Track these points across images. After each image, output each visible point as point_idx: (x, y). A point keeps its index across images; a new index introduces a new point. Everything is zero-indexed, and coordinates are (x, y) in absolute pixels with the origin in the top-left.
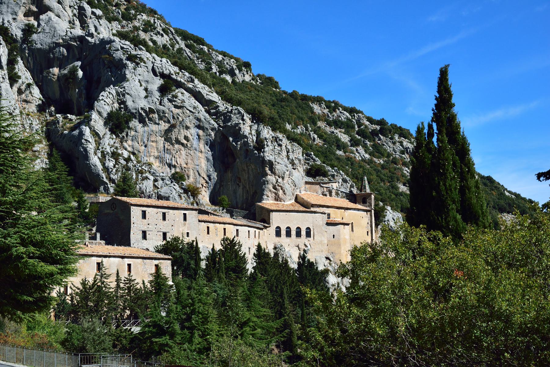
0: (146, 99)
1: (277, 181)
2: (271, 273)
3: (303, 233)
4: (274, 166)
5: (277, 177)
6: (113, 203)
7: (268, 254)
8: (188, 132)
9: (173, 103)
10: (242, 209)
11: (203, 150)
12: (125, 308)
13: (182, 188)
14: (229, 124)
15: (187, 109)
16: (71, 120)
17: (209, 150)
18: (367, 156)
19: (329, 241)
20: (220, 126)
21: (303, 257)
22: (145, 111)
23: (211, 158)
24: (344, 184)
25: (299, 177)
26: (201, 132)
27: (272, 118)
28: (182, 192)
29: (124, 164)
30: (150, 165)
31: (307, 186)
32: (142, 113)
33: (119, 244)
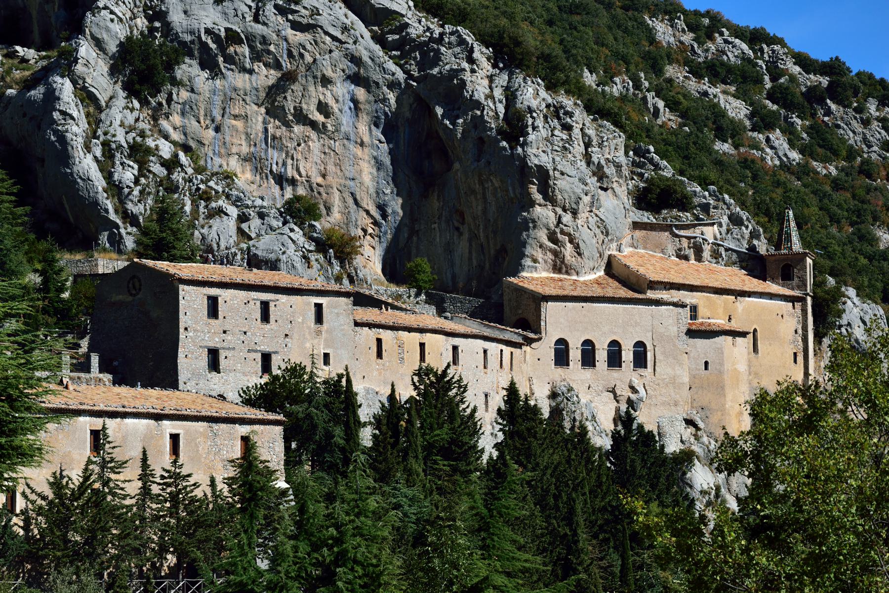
0: (220, 7)
1: (559, 221)
2: (544, 461)
3: (627, 356)
4: (551, 183)
5: (559, 211)
6: (134, 277)
7: (536, 410)
8: (328, 94)
9: (290, 17)
10: (468, 293)
11: (366, 139)
12: (162, 550)
13: (311, 239)
14: (435, 71)
15: (327, 33)
16: (24, 60)
17: (383, 139)
18: (795, 156)
19: (693, 377)
20: (410, 76)
21: (625, 420)
22: (216, 38)
23: (387, 161)
24: (736, 230)
25: (617, 212)
26: (361, 93)
27: (546, 58)
28: (312, 248)
29: (162, 175)
30: (228, 177)
31: (638, 234)
32: (209, 41)
33: (149, 383)
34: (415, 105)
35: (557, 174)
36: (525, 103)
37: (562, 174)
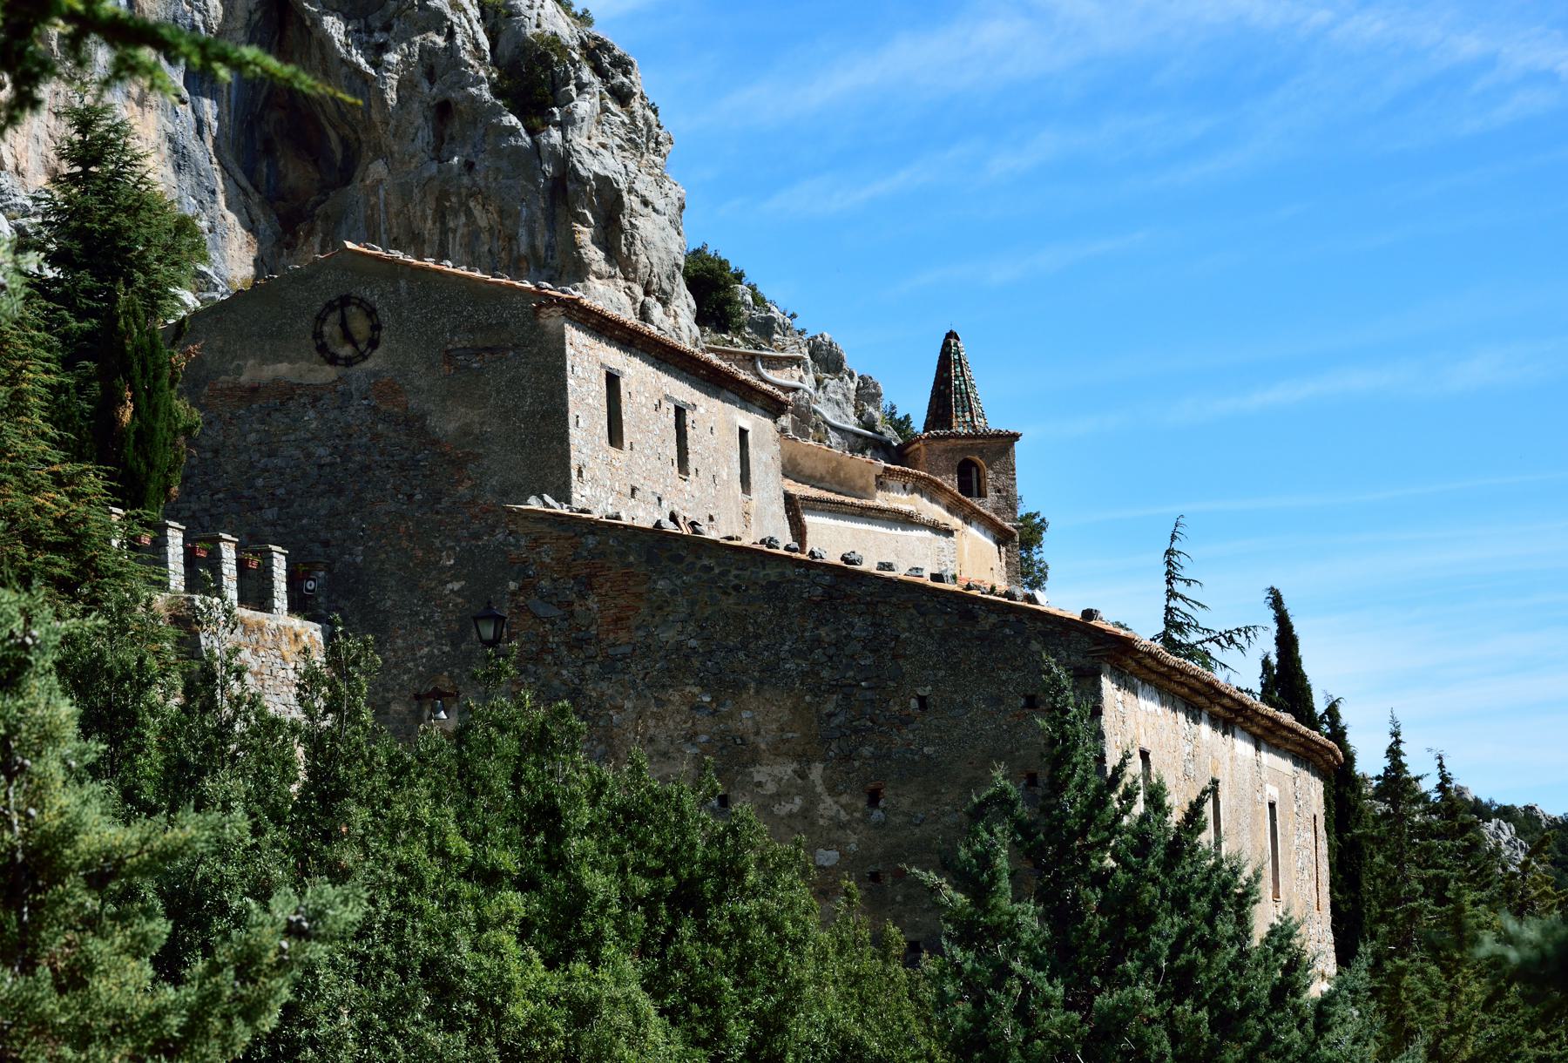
4: (625, 222)
6: (345, 301)
17: (185, 94)
23: (202, 152)
24: (832, 383)
34: (256, 17)
35: (636, 203)
36: (545, 26)
37: (646, 203)
